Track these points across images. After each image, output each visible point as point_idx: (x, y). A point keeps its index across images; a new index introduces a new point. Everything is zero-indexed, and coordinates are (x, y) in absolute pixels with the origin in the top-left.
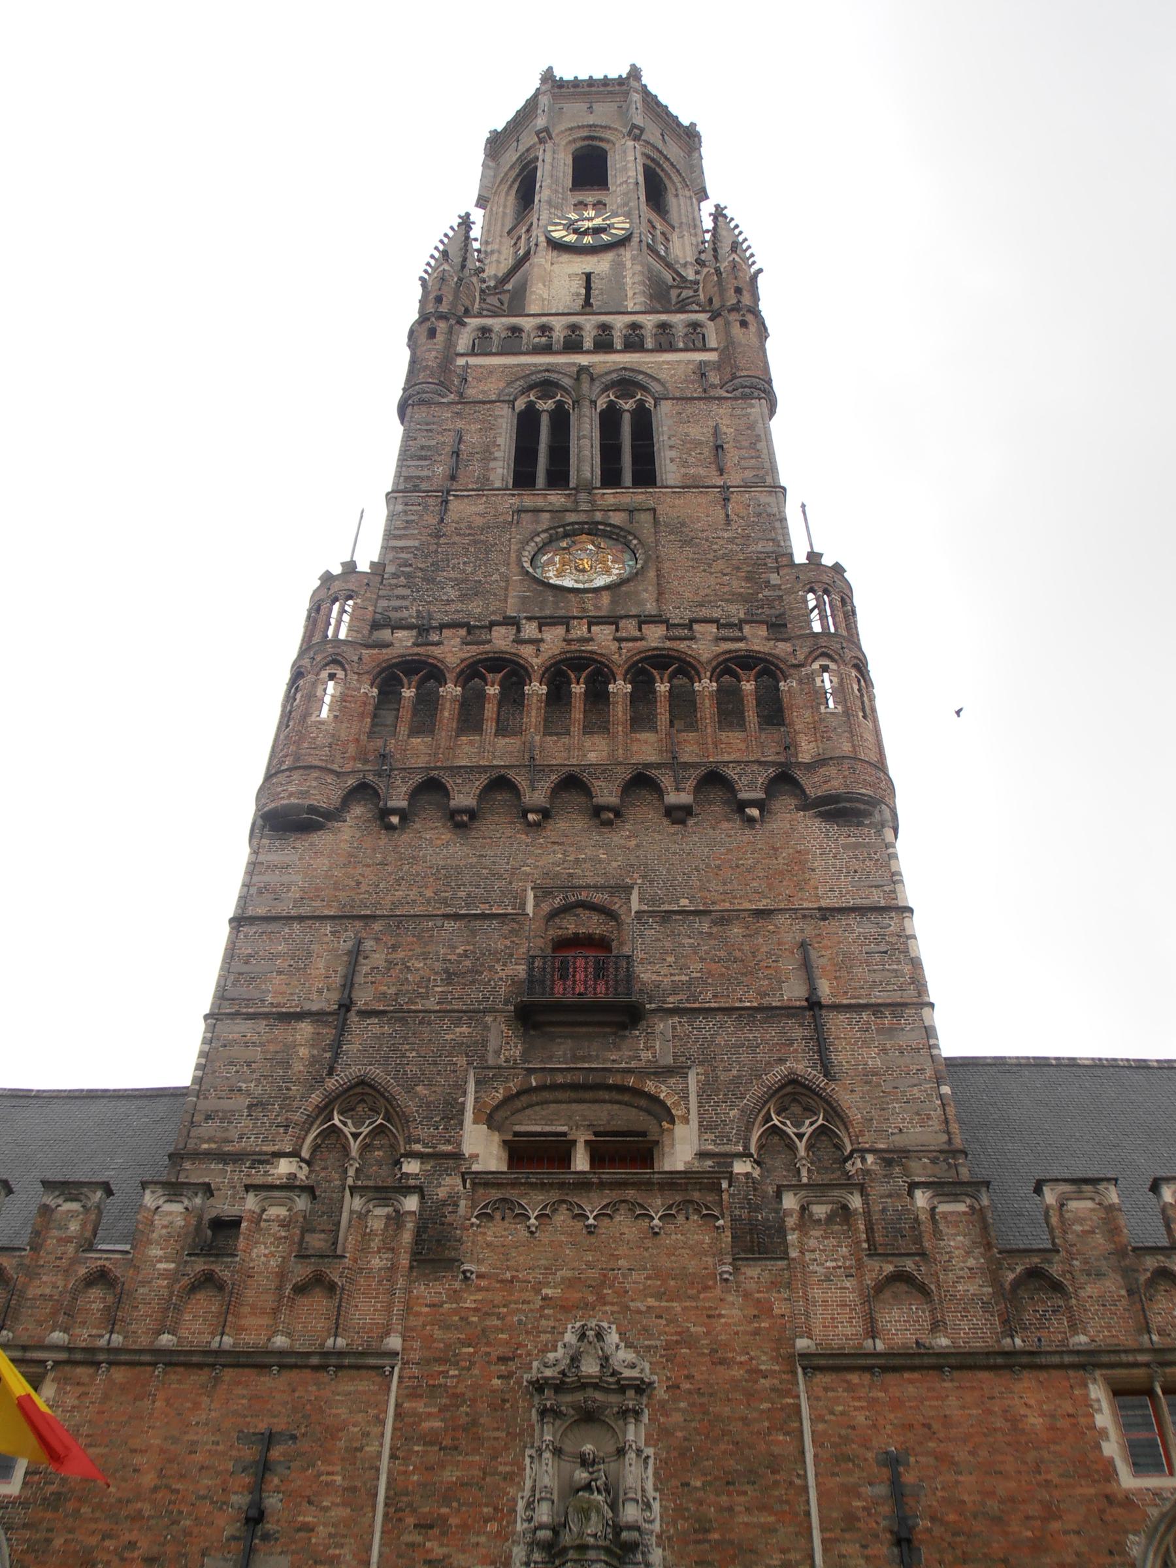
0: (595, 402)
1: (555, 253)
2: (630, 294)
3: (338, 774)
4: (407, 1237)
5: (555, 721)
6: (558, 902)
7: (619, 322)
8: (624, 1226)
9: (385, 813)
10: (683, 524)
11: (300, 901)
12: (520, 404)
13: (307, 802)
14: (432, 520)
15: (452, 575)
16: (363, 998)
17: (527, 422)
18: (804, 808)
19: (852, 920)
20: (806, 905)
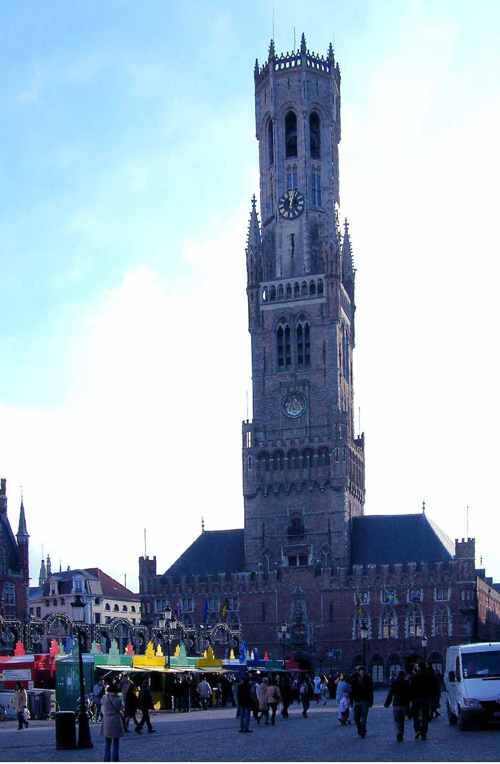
0: (294, 329)
1: (282, 220)
2: (305, 251)
3: (255, 485)
4: (276, 577)
5: (289, 468)
6: (292, 512)
7: (299, 280)
8: (302, 573)
9: (264, 494)
10: (315, 386)
11: (254, 514)
12: (278, 328)
13: (251, 493)
14: (262, 389)
15: (268, 411)
16: (266, 534)
17: (280, 333)
18: (331, 487)
19: (336, 513)
20: (330, 511)
